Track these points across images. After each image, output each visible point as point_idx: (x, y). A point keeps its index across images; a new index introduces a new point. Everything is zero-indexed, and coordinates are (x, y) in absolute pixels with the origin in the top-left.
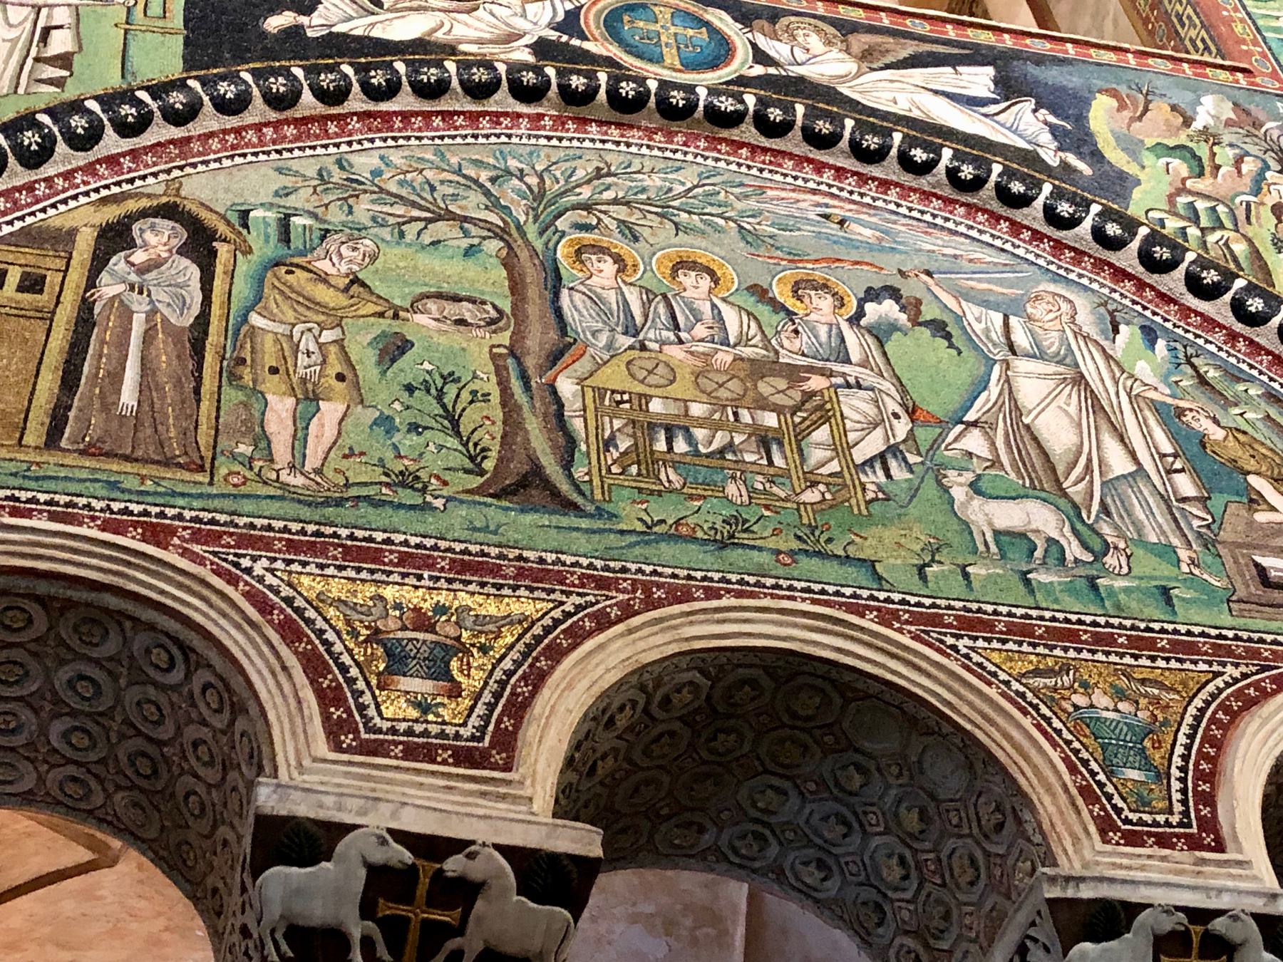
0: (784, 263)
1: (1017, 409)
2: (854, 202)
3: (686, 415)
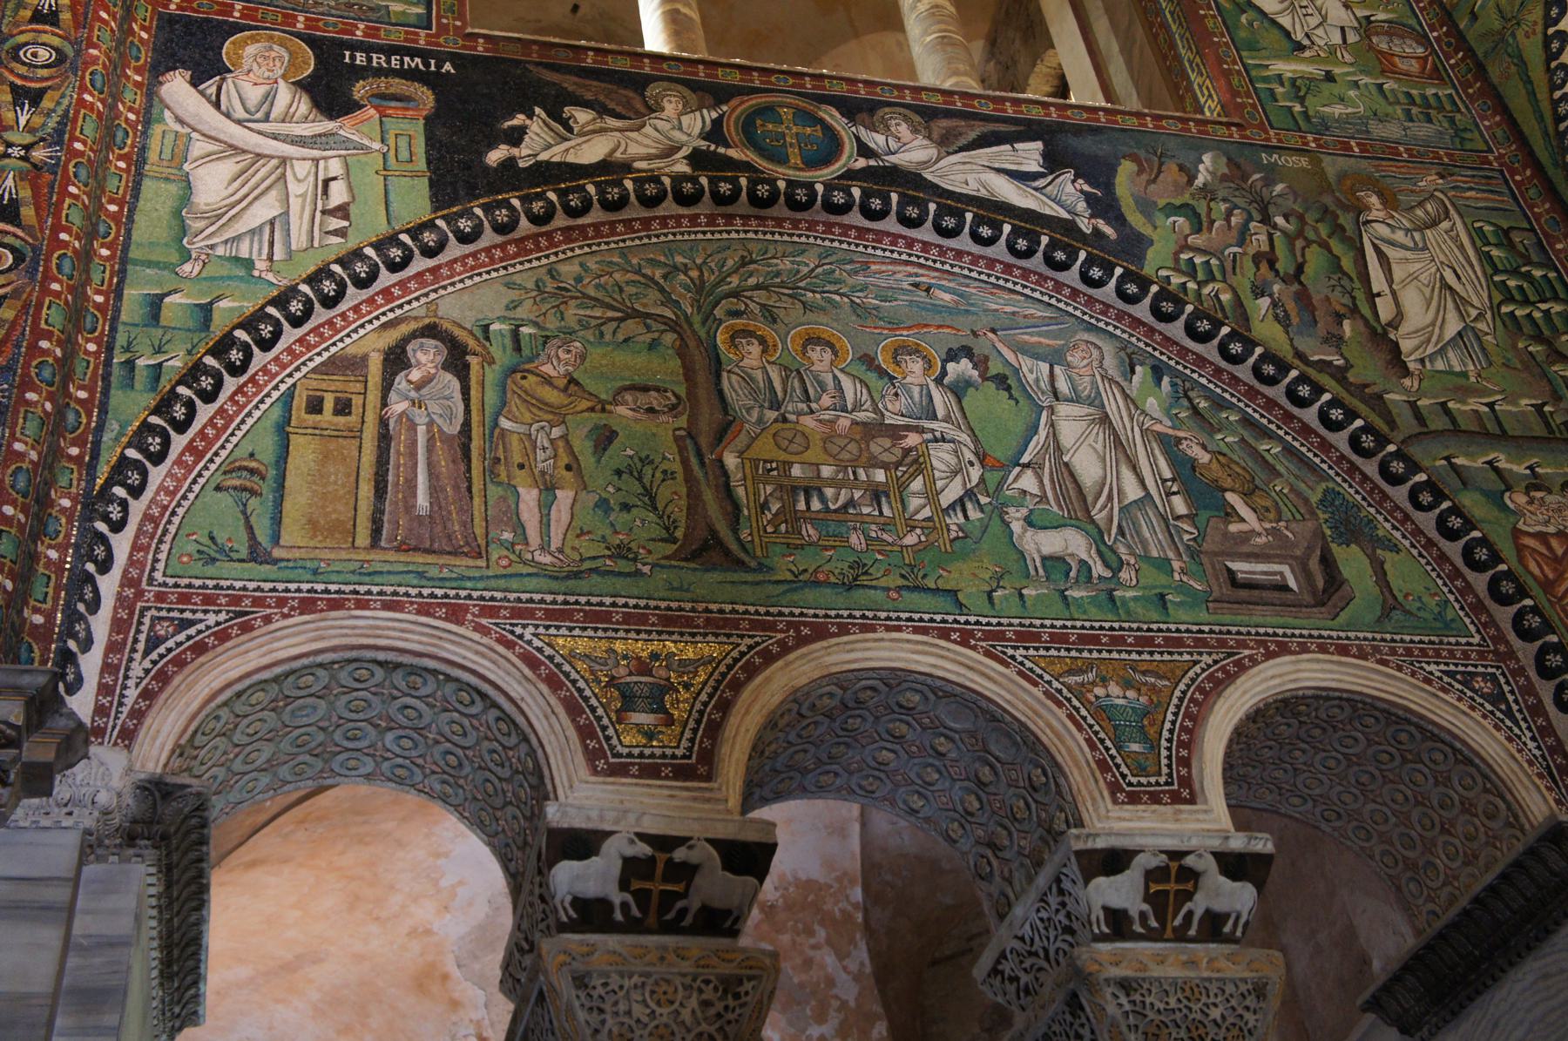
1: (1059, 448)
2: (937, 270)
3: (819, 476)
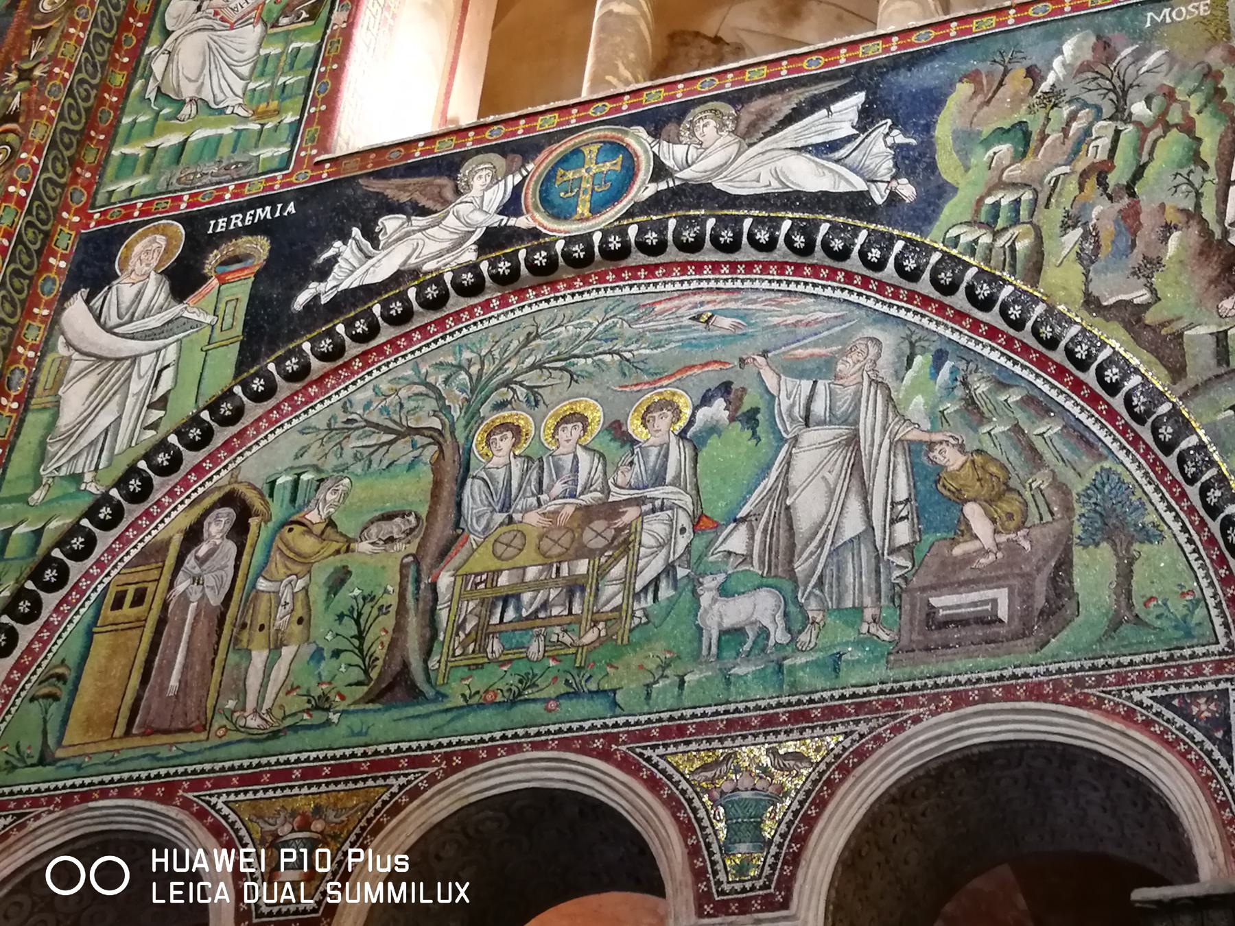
0: (646, 387)
2: (728, 290)
